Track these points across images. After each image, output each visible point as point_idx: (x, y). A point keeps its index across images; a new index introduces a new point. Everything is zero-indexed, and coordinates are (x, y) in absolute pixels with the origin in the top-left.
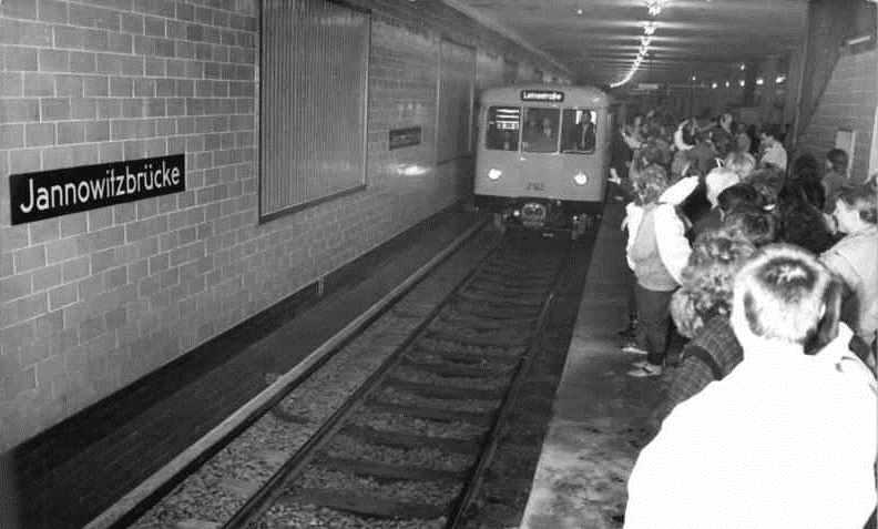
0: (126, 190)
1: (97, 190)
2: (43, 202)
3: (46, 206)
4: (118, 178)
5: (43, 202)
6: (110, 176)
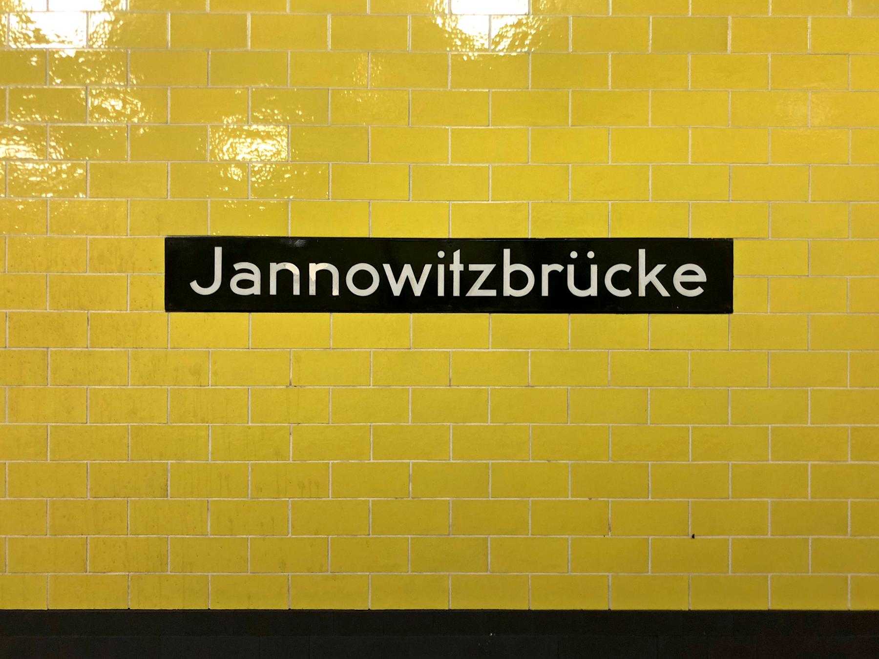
2: (244, 284)
3: (256, 290)
4: (473, 267)
5: (244, 284)
6: (448, 261)
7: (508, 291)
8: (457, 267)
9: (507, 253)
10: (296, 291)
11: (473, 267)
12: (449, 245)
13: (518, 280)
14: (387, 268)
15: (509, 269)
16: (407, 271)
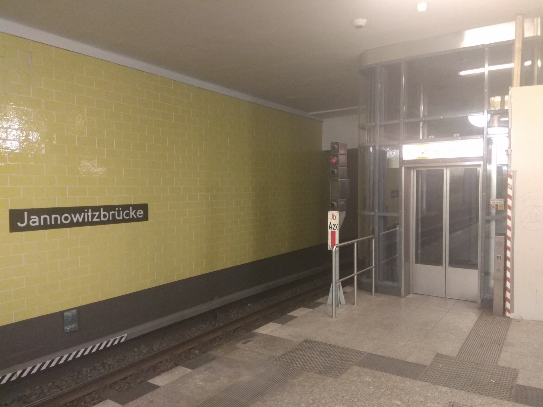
0: (100, 218)
1: (78, 218)
3: (37, 224)
4: (94, 213)
6: (88, 212)
7: (102, 219)
8: (90, 214)
9: (102, 209)
10: (49, 223)
11: (94, 213)
12: (88, 208)
13: (105, 216)
14: (73, 215)
15: (102, 213)
16: (78, 215)
